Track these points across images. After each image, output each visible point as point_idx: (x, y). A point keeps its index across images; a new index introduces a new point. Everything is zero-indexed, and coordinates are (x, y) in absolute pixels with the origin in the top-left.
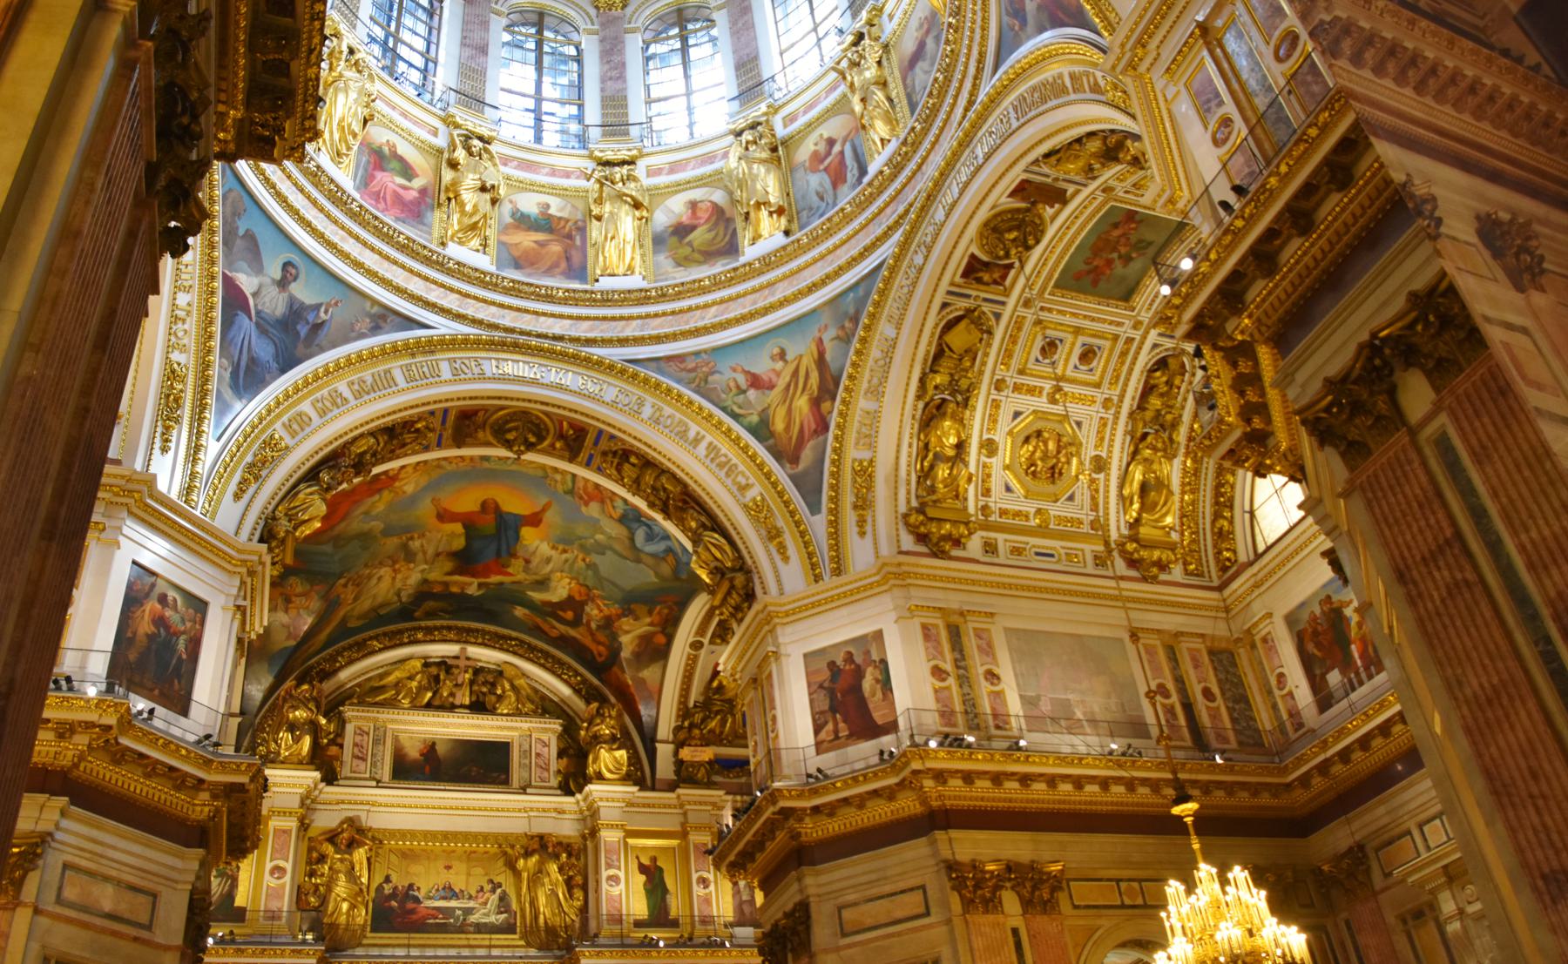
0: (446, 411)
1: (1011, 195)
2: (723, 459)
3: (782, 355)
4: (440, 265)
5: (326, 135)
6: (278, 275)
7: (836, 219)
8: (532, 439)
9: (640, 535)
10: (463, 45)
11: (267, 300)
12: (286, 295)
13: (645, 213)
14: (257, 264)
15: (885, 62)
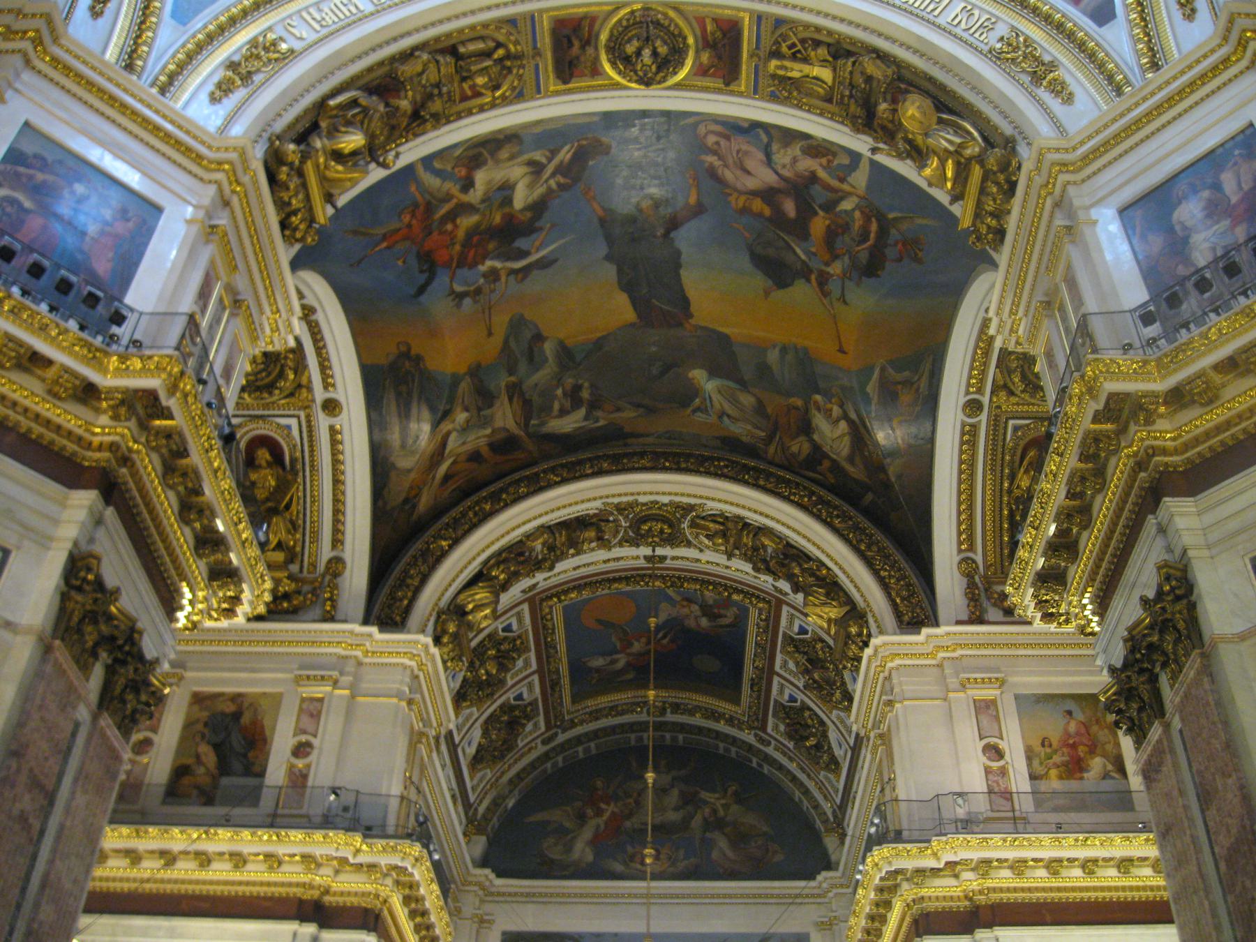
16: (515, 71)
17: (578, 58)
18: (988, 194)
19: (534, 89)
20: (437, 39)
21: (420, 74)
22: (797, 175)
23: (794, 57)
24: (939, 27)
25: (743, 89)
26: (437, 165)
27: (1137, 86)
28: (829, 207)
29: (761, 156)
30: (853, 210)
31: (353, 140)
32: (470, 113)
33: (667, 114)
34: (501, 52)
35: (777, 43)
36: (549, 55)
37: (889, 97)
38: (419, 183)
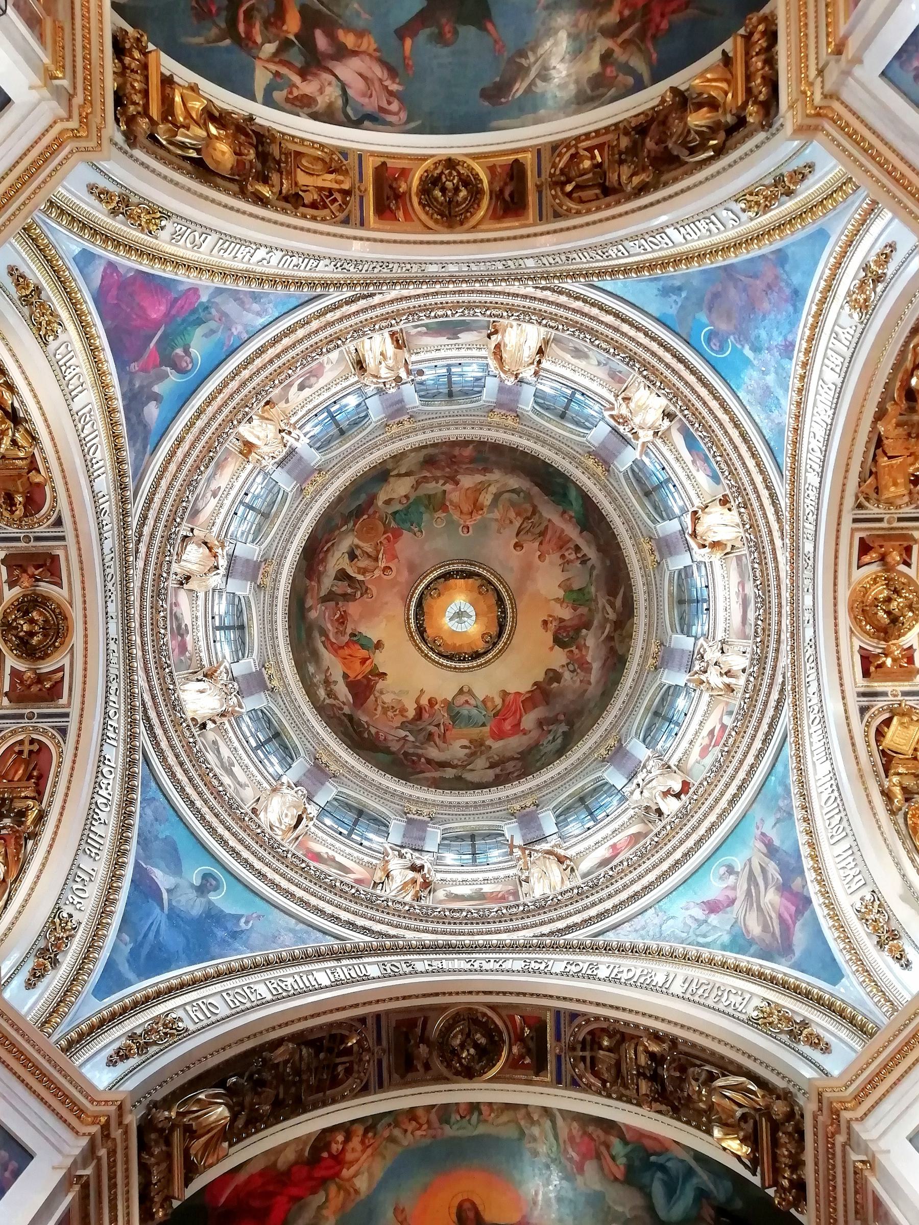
0: (378, 1016)
1: (859, 567)
2: (705, 987)
3: (731, 870)
4: (370, 902)
5: (262, 816)
6: (196, 881)
7: (731, 741)
8: (483, 1041)
9: (658, 1190)
10: (404, 836)
11: (183, 899)
12: (203, 900)
13: (568, 862)
14: (175, 864)
15: (726, 647)
16: (558, 172)
17: (506, 184)
18: (140, 92)
19: (542, 152)
20: (618, 203)
21: (634, 174)
22: (315, 75)
23: (330, 191)
24: (216, 231)
25: (371, 159)
26: (630, 80)
27: (36, 212)
28: (286, 44)
29: (350, 92)
30: (263, 44)
31: (698, 120)
32: (597, 132)
33: (433, 131)
34: (569, 188)
35: (346, 203)
36: (530, 185)
37: (248, 166)
38: (649, 63)
